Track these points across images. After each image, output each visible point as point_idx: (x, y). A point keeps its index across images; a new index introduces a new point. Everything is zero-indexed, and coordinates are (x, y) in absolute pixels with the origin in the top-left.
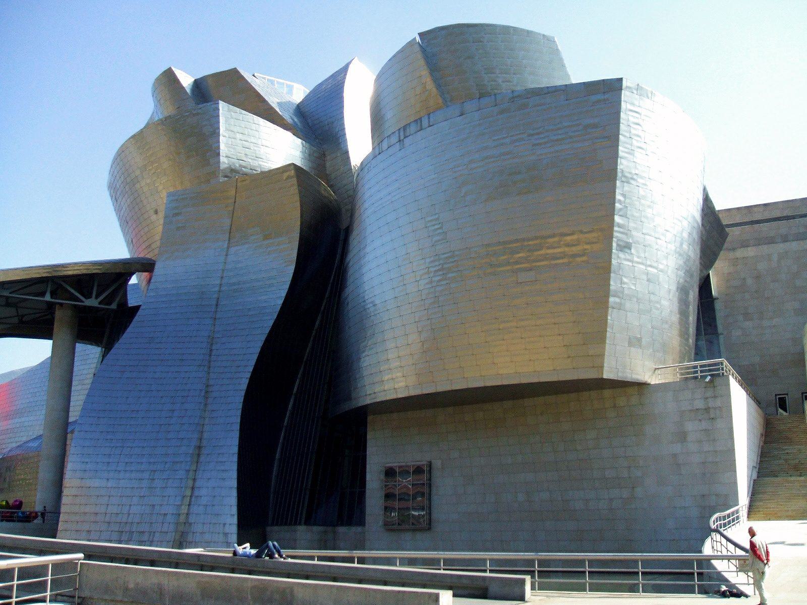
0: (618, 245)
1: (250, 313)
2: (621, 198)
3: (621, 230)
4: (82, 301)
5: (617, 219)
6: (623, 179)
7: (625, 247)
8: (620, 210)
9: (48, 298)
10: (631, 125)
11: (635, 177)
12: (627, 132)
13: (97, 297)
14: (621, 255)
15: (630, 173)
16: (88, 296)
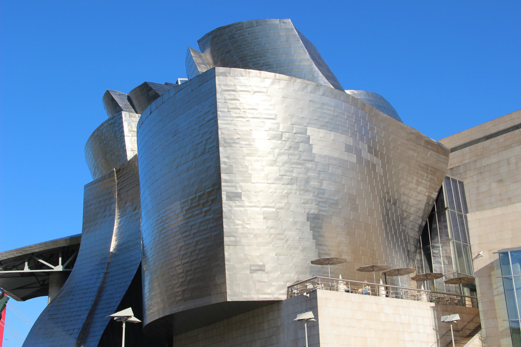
0: (227, 196)
1: (126, 266)
2: (226, 160)
3: (229, 184)
4: (53, 269)
5: (223, 176)
6: (226, 145)
7: (234, 197)
8: (226, 169)
9: (27, 270)
10: (228, 101)
11: (237, 141)
12: (224, 108)
13: (62, 265)
14: (232, 203)
15: (231, 139)
16: (56, 264)
